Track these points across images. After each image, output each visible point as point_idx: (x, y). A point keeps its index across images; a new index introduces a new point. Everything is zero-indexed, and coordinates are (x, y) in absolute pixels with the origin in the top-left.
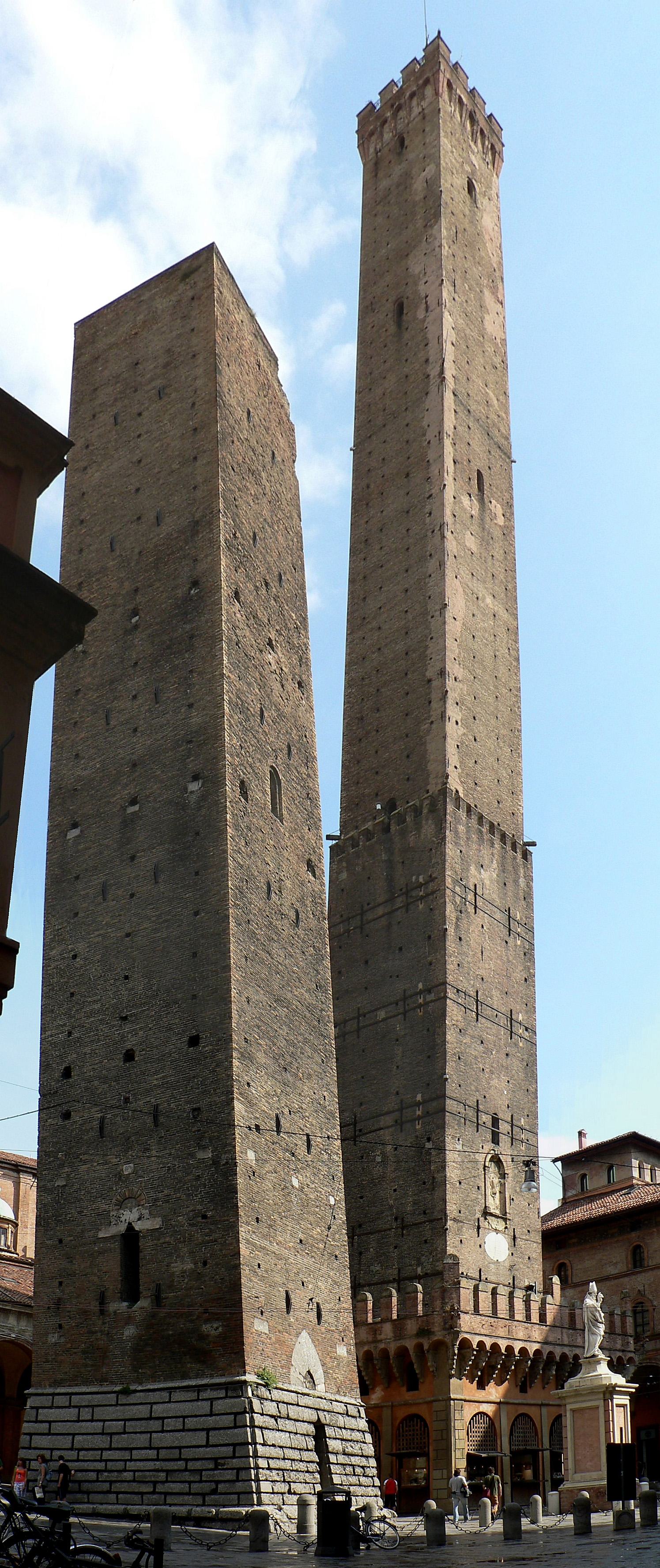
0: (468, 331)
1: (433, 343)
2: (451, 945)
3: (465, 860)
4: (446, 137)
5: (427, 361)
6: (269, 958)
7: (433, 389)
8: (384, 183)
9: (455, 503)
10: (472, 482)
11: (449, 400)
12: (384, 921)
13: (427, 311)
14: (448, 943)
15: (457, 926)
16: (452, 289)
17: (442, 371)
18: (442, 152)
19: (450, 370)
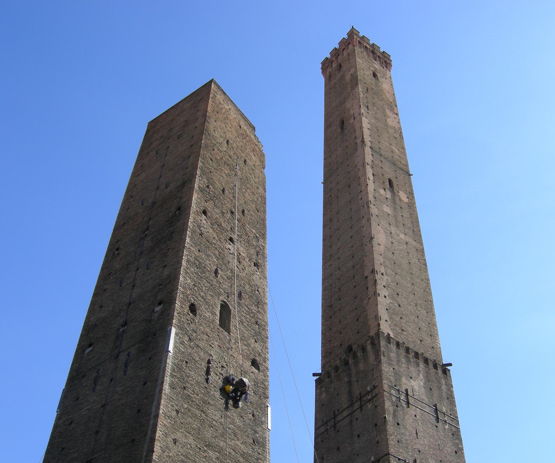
0: (377, 124)
1: (358, 131)
2: (391, 428)
3: (398, 376)
4: (359, 58)
5: (356, 138)
6: (203, 415)
7: (359, 148)
8: (333, 82)
9: (375, 193)
10: (385, 183)
11: (368, 150)
12: (347, 420)
13: (354, 118)
14: (388, 427)
15: (395, 416)
16: (366, 109)
17: (363, 138)
18: (357, 64)
19: (367, 139)
